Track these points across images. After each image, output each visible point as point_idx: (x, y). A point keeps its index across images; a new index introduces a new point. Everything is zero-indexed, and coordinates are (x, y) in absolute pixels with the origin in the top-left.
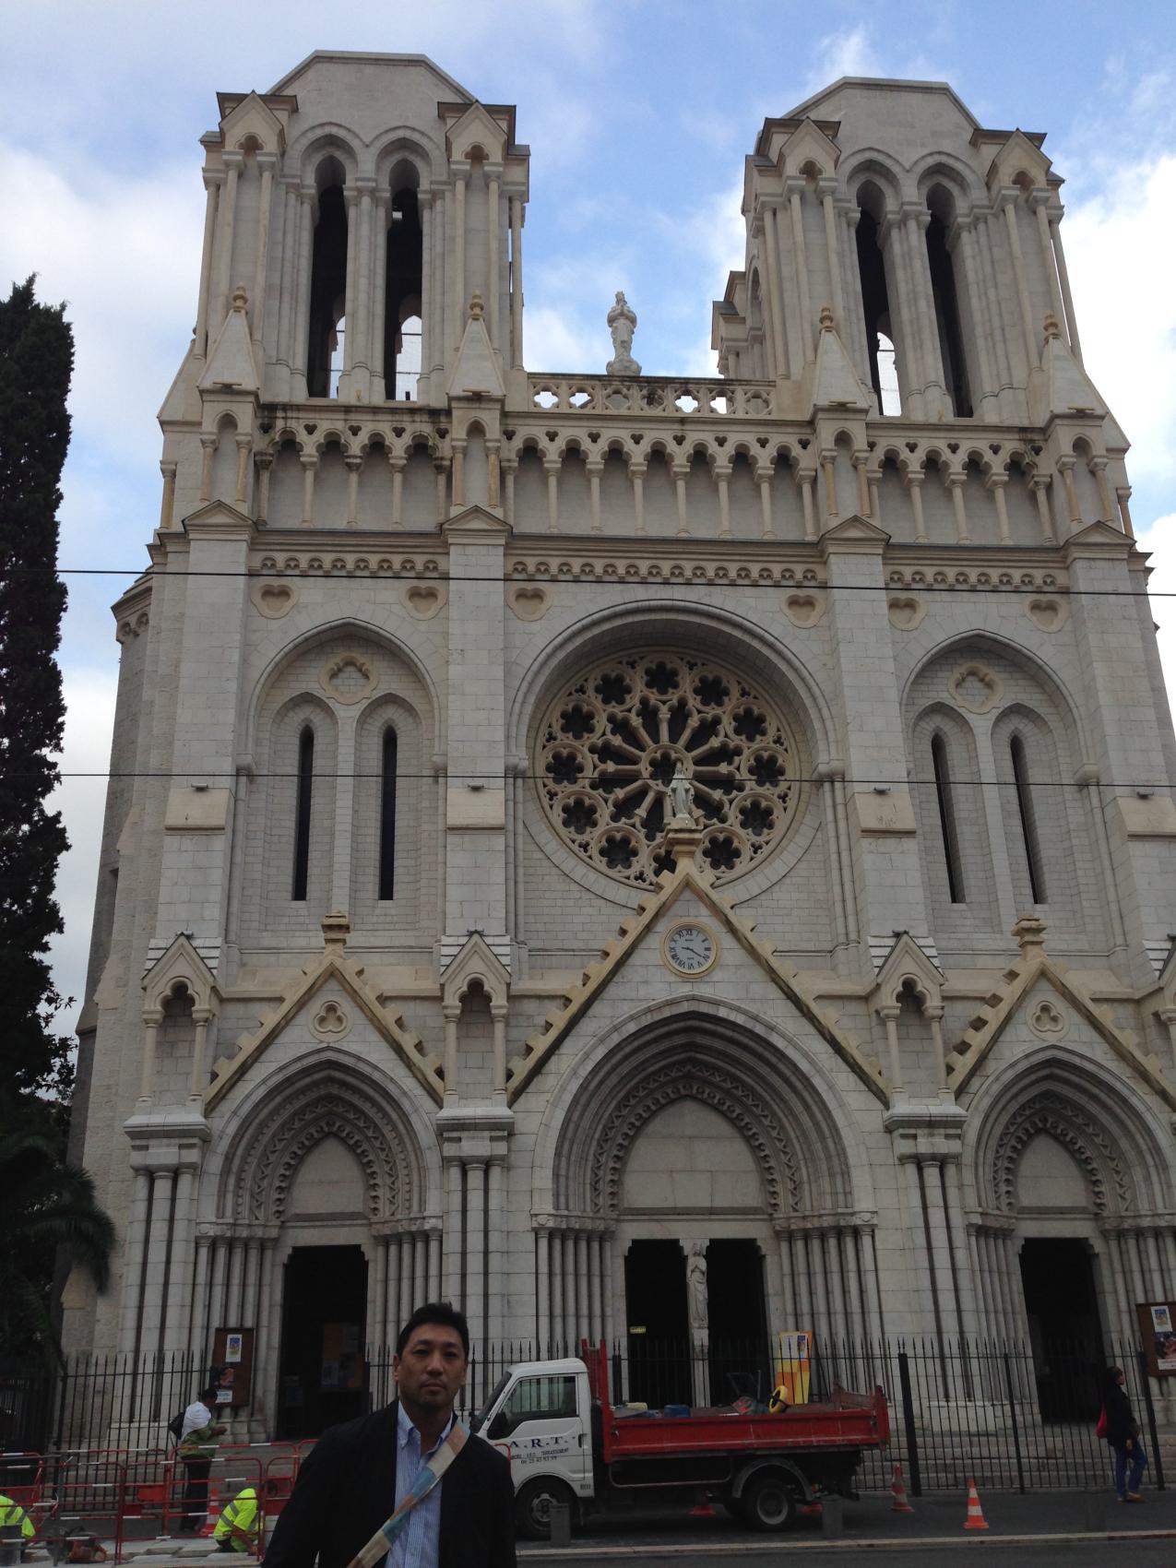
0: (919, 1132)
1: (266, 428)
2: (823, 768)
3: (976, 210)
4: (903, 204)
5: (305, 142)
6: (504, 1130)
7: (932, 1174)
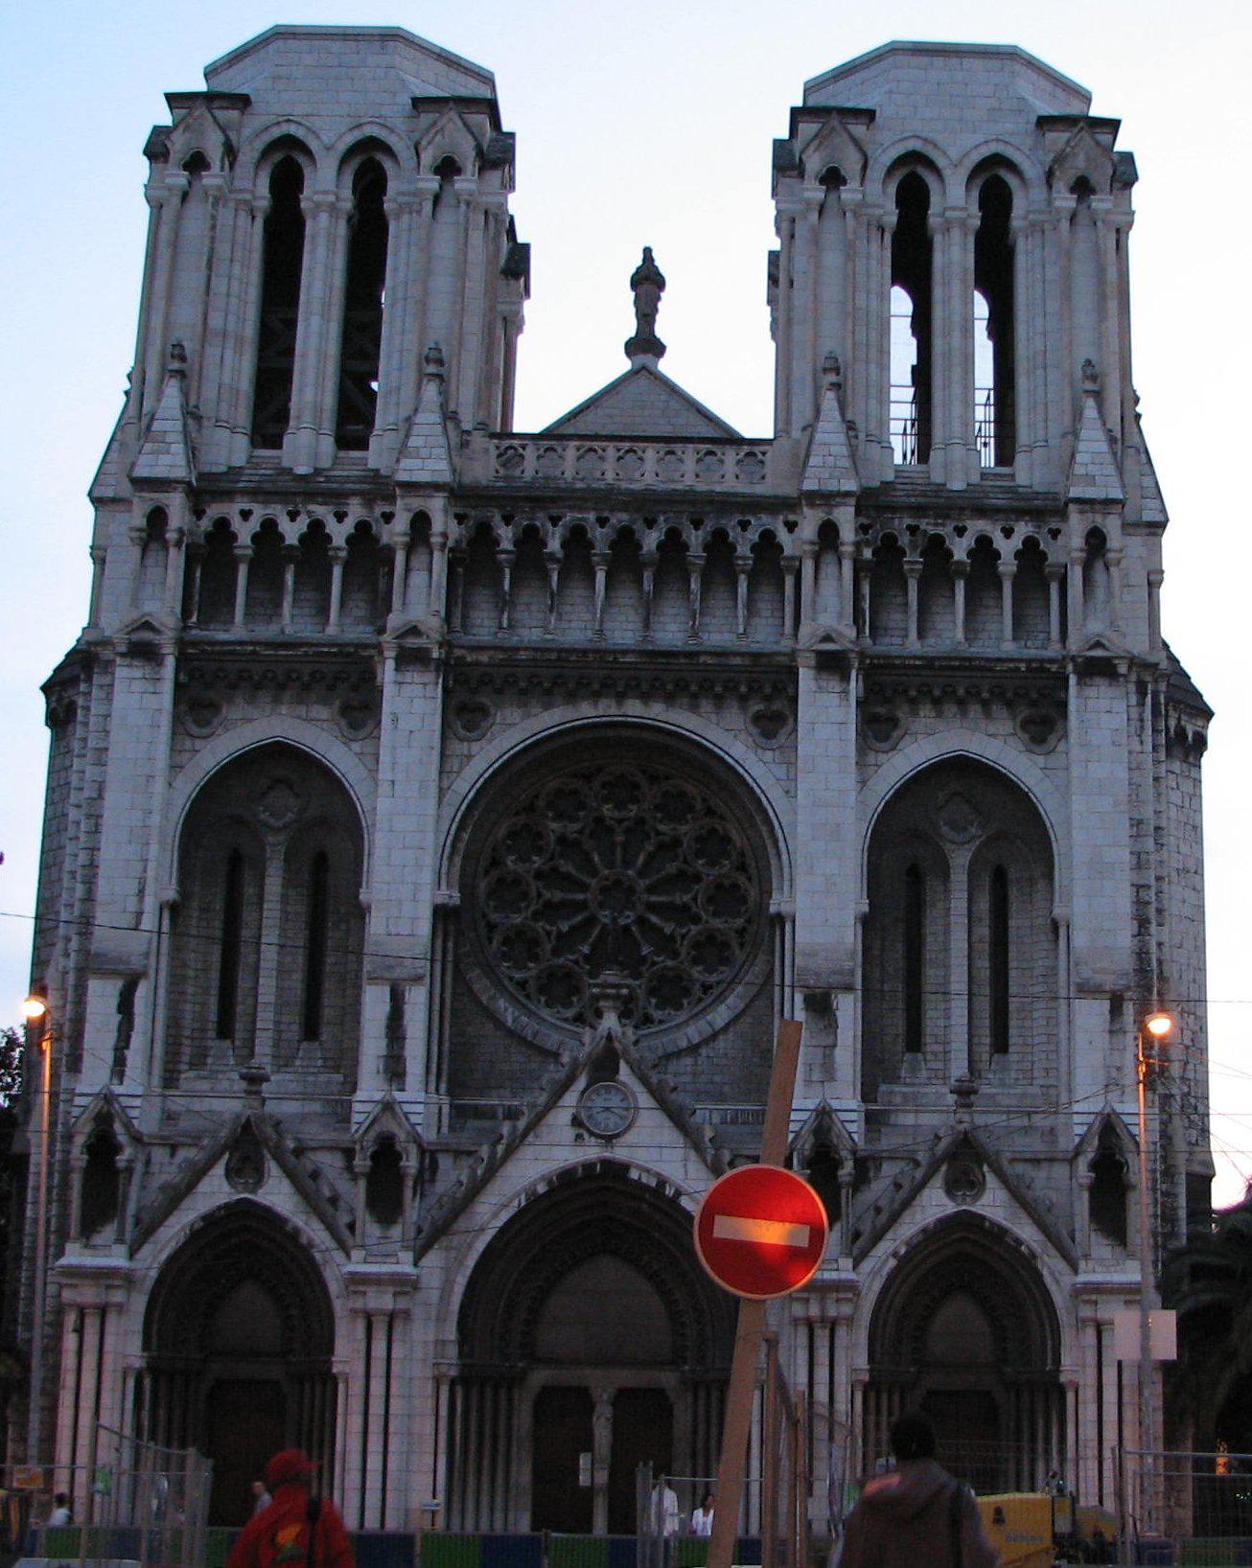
0: (813, 1296)
1: (198, 513)
2: (773, 909)
3: (1031, 216)
4: (945, 209)
5: (260, 144)
6: (405, 1285)
7: (822, 1337)
